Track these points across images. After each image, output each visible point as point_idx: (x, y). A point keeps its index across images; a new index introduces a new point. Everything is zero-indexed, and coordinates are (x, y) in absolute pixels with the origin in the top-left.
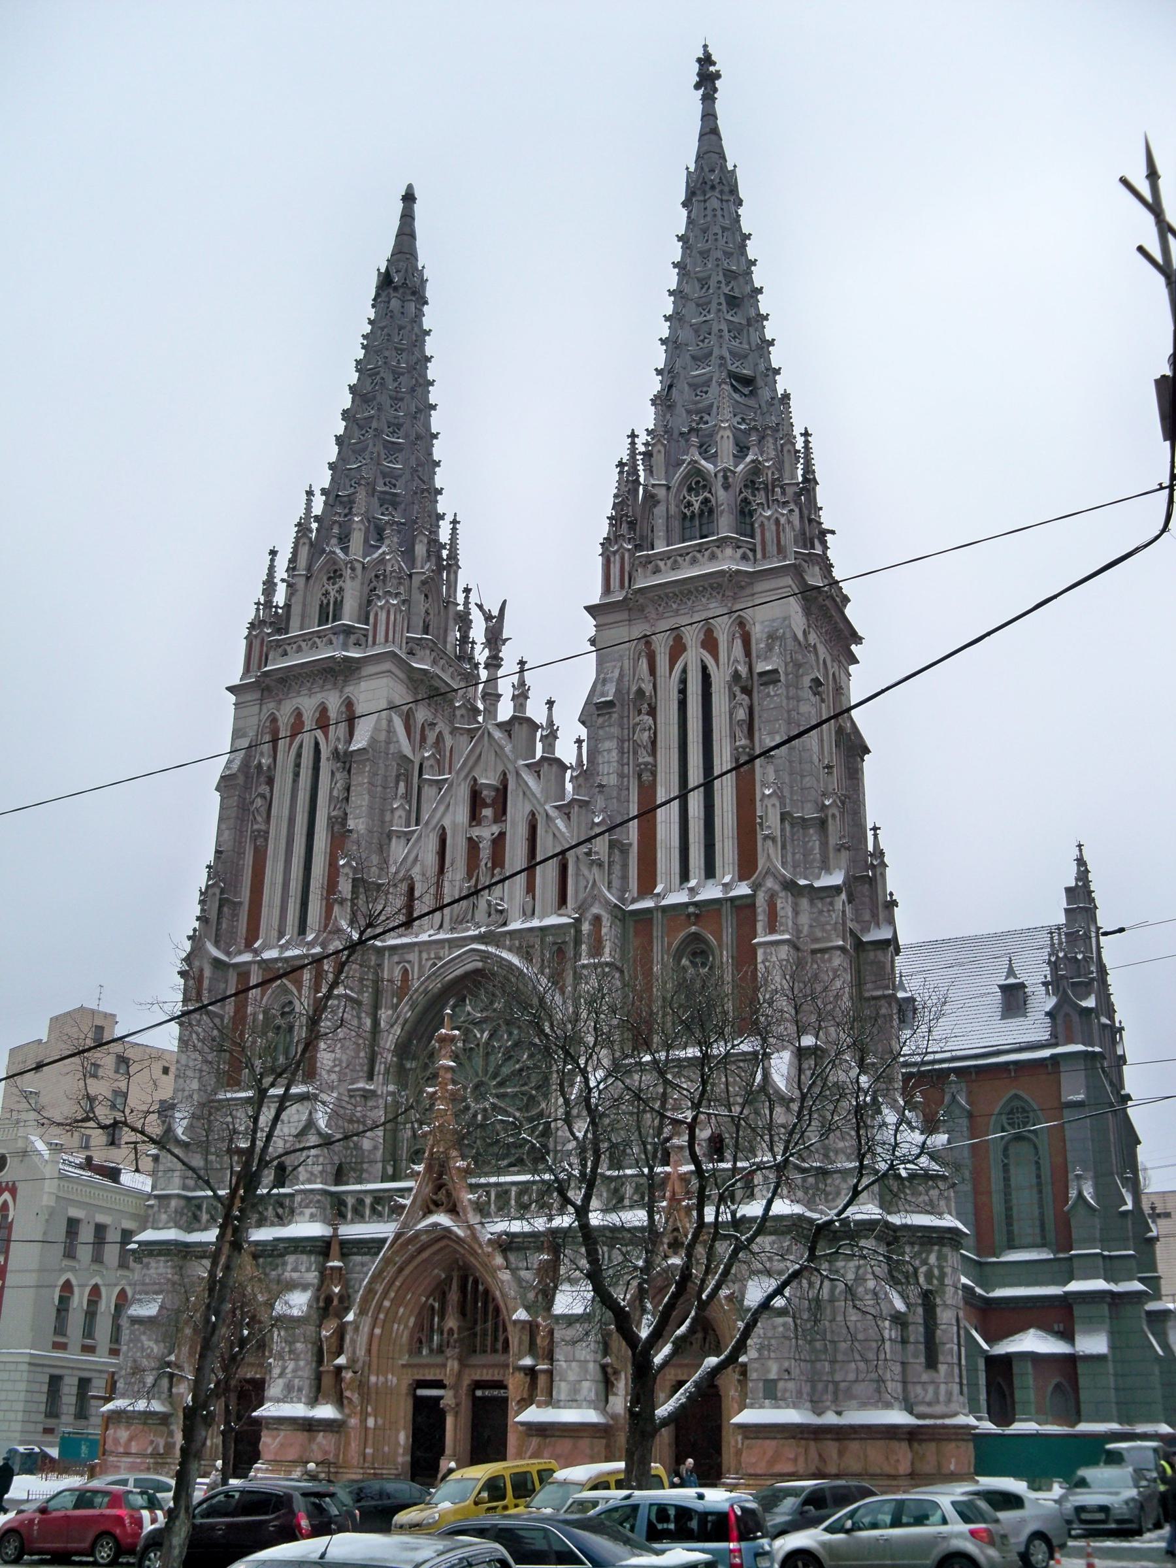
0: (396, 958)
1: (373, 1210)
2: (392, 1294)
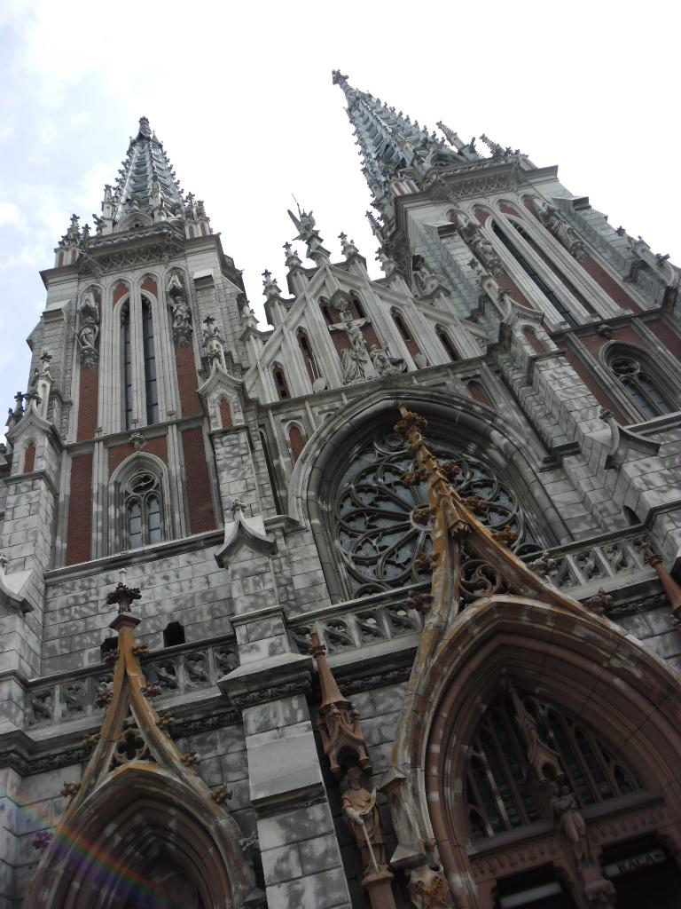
0: (282, 417)
1: (365, 631)
2: (440, 733)
